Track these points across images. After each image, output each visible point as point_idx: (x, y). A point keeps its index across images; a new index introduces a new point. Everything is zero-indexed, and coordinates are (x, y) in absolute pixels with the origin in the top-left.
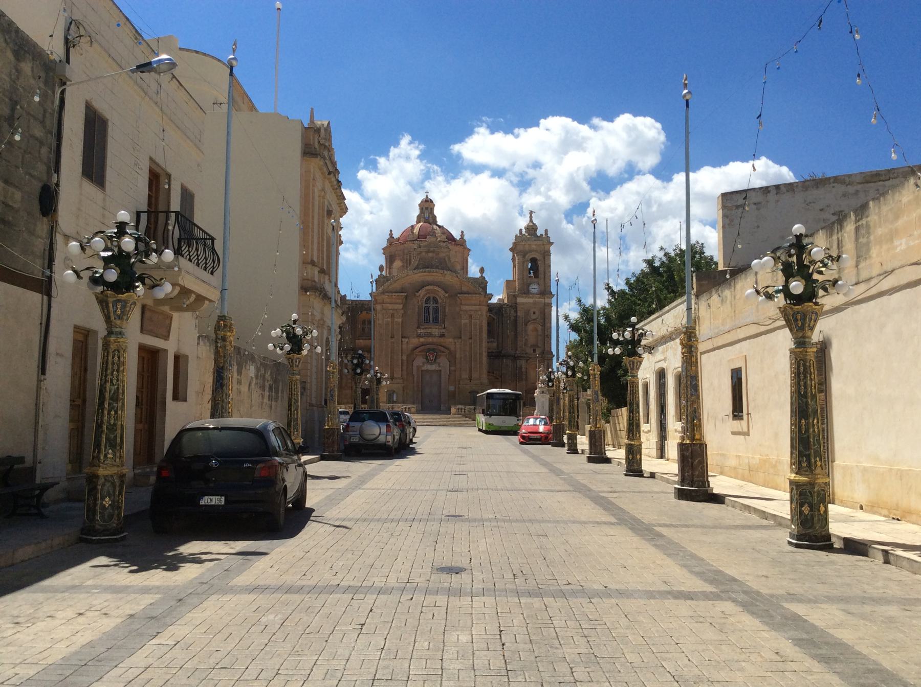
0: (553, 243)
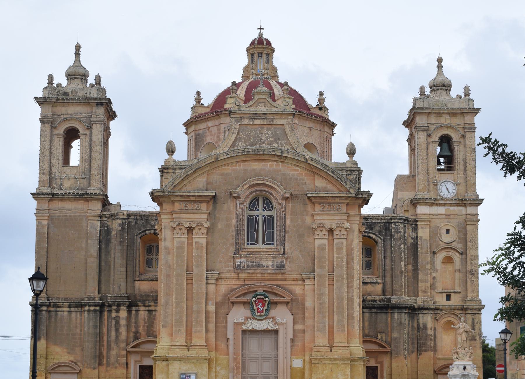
0: (478, 109)
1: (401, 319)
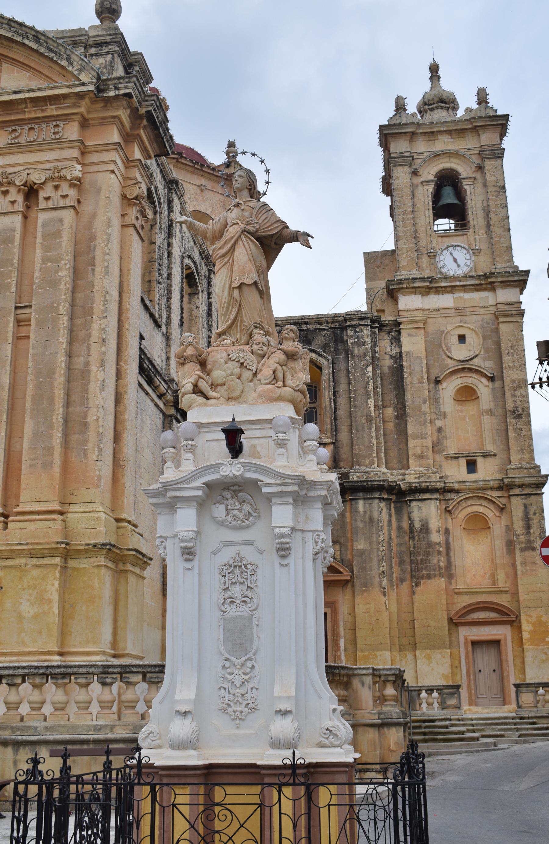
1: (371, 511)
